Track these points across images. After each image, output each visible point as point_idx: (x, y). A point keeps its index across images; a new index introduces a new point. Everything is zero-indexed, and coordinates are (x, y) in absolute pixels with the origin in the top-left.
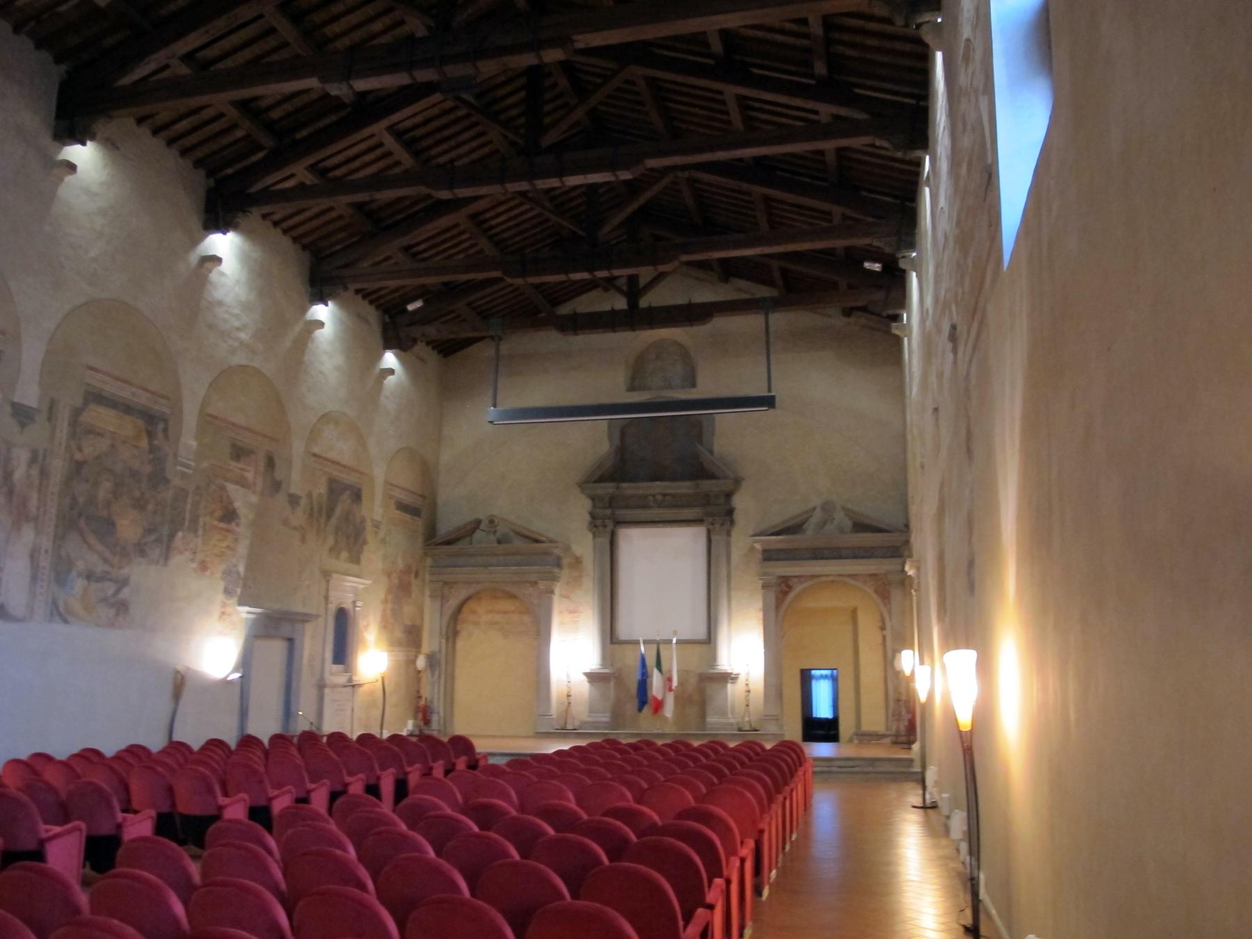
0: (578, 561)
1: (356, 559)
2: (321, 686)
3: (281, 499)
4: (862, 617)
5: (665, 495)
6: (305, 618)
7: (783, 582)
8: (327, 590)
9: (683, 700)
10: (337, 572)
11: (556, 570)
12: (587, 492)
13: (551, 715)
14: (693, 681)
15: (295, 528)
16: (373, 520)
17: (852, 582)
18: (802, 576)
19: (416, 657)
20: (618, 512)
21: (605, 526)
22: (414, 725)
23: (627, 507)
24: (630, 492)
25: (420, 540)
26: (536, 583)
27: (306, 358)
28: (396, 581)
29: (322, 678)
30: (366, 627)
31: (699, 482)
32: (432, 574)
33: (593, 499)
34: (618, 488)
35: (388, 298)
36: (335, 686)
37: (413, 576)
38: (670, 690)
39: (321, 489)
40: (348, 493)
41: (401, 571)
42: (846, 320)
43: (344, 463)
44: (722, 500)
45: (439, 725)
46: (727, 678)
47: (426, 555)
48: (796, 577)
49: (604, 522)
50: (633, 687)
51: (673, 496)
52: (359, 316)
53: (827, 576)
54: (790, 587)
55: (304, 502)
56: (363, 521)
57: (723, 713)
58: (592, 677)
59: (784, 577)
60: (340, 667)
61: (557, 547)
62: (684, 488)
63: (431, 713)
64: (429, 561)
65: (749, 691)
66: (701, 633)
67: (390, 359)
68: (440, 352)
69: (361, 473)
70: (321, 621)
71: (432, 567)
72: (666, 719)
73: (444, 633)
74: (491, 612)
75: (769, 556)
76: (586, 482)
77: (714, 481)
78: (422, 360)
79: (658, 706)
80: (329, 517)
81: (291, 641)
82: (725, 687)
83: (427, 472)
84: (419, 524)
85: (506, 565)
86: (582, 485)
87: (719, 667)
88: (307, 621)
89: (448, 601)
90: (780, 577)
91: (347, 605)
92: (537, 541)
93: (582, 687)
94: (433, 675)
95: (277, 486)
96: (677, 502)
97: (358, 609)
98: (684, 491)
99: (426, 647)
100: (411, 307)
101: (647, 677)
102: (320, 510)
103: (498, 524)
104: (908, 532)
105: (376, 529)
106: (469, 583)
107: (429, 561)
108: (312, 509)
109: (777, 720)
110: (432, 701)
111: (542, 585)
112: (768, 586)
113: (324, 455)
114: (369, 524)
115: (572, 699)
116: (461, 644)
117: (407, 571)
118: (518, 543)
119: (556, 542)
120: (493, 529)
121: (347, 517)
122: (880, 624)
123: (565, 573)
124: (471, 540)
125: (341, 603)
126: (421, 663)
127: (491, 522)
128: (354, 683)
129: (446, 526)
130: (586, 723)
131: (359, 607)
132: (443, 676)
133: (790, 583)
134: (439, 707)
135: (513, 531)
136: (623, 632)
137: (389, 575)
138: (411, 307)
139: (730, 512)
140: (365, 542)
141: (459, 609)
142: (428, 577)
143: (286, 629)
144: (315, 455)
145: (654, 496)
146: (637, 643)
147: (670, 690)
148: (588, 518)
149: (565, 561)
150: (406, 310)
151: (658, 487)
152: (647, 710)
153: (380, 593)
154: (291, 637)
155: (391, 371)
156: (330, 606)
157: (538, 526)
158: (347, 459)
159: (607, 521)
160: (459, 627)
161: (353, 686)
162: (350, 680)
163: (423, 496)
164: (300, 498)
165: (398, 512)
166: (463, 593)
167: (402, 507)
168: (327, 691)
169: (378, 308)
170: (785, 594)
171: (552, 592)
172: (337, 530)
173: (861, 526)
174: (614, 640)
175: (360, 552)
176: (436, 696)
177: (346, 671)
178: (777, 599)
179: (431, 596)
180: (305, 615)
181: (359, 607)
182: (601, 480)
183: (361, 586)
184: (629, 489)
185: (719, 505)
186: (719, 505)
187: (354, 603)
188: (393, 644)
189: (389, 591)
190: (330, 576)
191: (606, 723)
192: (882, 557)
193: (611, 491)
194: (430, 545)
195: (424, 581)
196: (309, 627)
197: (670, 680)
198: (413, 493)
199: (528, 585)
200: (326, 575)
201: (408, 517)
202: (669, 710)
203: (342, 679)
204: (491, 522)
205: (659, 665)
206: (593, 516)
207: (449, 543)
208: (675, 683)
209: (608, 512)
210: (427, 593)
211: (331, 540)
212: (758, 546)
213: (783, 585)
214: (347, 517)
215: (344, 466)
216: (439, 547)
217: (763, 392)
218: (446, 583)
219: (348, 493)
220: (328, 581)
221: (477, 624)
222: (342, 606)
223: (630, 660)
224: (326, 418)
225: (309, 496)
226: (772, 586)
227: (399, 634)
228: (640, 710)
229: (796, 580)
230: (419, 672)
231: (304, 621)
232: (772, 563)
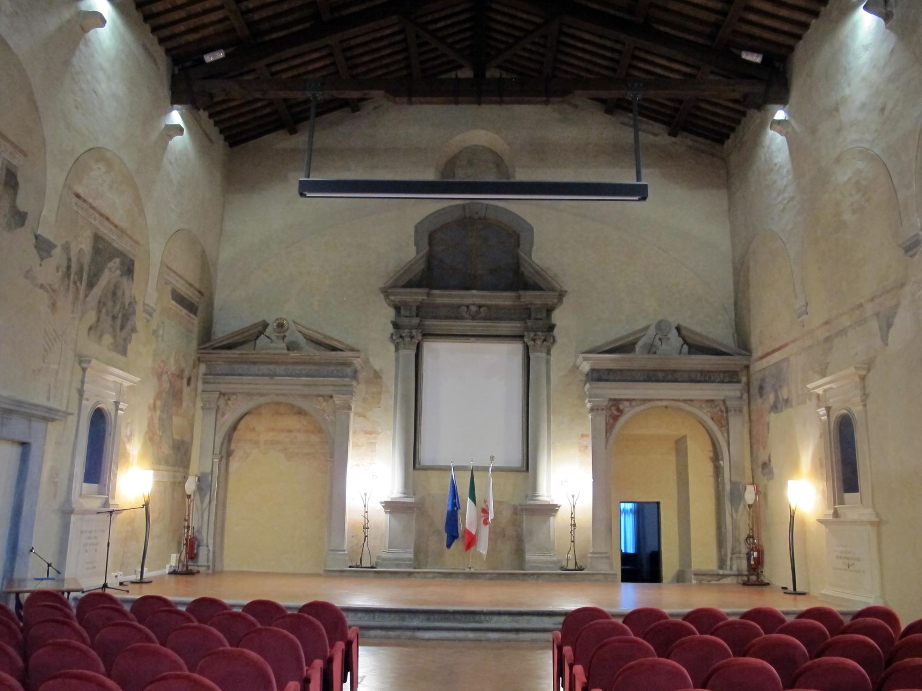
0: (377, 375)
1: (124, 352)
2: (66, 512)
3: (24, 237)
4: (690, 443)
5: (480, 306)
6: (48, 416)
7: (615, 405)
8: (83, 382)
9: (497, 535)
10: (97, 359)
11: (354, 383)
12: (392, 298)
13: (344, 551)
14: (507, 514)
15: (42, 286)
16: (145, 304)
17: (687, 407)
18: (634, 400)
19: (185, 478)
20: (428, 322)
21: (412, 337)
22: (179, 561)
23: (436, 317)
24: (439, 301)
25: (194, 345)
26: (331, 397)
27: (75, 61)
28: (166, 385)
29: (68, 500)
30: (129, 438)
31: (522, 293)
32: (205, 382)
33: (397, 309)
34: (428, 295)
35: (182, 40)
36: (85, 512)
37: (185, 381)
38: (486, 522)
39: (83, 245)
40: (117, 260)
41: (173, 374)
42: (673, 139)
43: (116, 222)
44: (544, 314)
45: (208, 561)
46: (551, 509)
47: (199, 360)
48: (627, 400)
49: (411, 332)
50: (440, 521)
51: (489, 307)
52: (146, 49)
53: (661, 400)
54: (621, 411)
55: (57, 252)
56: (133, 303)
57: (546, 549)
58: (391, 507)
59: (615, 400)
60: (94, 486)
61: (358, 357)
62: (504, 299)
63: (198, 546)
64: (203, 368)
65: (575, 525)
66: (516, 460)
67: (176, 117)
68: (226, 139)
69: (137, 243)
70: (71, 420)
71: (205, 374)
72: (481, 554)
73: (217, 451)
74: (273, 430)
75: (597, 376)
76: (394, 286)
77: (538, 293)
78: (211, 141)
79: (471, 541)
80: (91, 285)
81: (24, 445)
82: (549, 519)
83: (206, 267)
84: (196, 320)
85: (299, 376)
86: (386, 292)
87: (540, 498)
88: (53, 420)
89: (223, 415)
90: (610, 400)
91: (107, 406)
92: (334, 349)
93: (380, 517)
94: (202, 502)
95: (19, 218)
96: (493, 314)
97: (119, 412)
98: (501, 302)
99: (195, 467)
100: (209, 58)
101: (459, 508)
102: (81, 269)
103: (287, 330)
104: (751, 356)
105: (148, 317)
106: (249, 395)
107: (203, 368)
108: (69, 267)
109: (608, 558)
110: (199, 531)
111: (338, 400)
112: (598, 409)
113: (90, 200)
114: (139, 309)
115: (370, 533)
116: (234, 465)
117: (180, 376)
118: (311, 352)
119: (358, 351)
120: (282, 334)
121: (114, 292)
122: (711, 454)
123: (361, 389)
124: (255, 345)
125: (98, 403)
126: (190, 486)
127: (280, 326)
128: (111, 509)
129: (225, 327)
130: (384, 559)
131: (121, 410)
132: (214, 503)
133: (621, 407)
134: (207, 538)
135: (306, 336)
136: (427, 456)
137: (160, 376)
138: (209, 58)
139: (551, 328)
140: (134, 330)
141: (234, 428)
142: (200, 386)
143: (18, 428)
144: (78, 196)
145: (468, 307)
146: (447, 469)
147: (486, 522)
148: (391, 329)
149: (362, 375)
150: (203, 62)
151: (473, 297)
152: (458, 545)
153: (148, 395)
154: (26, 440)
155: (179, 130)
156: (84, 402)
157: (333, 333)
158: (119, 217)
159: (414, 332)
160: (233, 446)
161: (111, 512)
162: (106, 504)
163: (200, 292)
164: (52, 246)
165: (174, 303)
166: (244, 406)
167: (179, 298)
168: (73, 518)
169: (168, 51)
170: (615, 418)
171: (350, 408)
172: (101, 304)
173: (696, 348)
174: (417, 466)
175: (127, 340)
176: (205, 526)
177: (101, 493)
178: (607, 424)
179: (203, 408)
180: (50, 410)
181: (121, 410)
182: (409, 285)
183: (126, 384)
184: (442, 297)
185: (541, 319)
186: (541, 319)
187: (117, 404)
188: (159, 462)
189: (158, 396)
190: (89, 362)
191: (410, 560)
192: (719, 382)
193: (420, 298)
194: (204, 349)
195: (196, 390)
196: (53, 429)
197: (485, 511)
198: (191, 285)
199: (321, 399)
200: (82, 361)
201: (184, 312)
202: (483, 547)
203: (95, 503)
204: (280, 326)
205: (473, 496)
206: (396, 325)
207: (229, 347)
208: (491, 516)
209: (416, 321)
210: (199, 404)
211: (91, 317)
212: (586, 367)
213: (613, 408)
214: (114, 292)
215: (116, 226)
216: (216, 351)
217: (633, 181)
218: (222, 394)
219: (117, 260)
220: (84, 370)
221: (256, 443)
222: (99, 406)
223: (438, 488)
224: (97, 154)
225: (66, 248)
226: (602, 409)
227: (166, 450)
228: (449, 546)
229: (627, 404)
230: (189, 496)
231: (46, 420)
232: (602, 384)
